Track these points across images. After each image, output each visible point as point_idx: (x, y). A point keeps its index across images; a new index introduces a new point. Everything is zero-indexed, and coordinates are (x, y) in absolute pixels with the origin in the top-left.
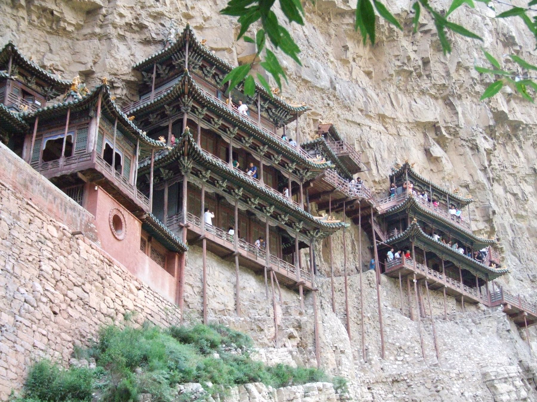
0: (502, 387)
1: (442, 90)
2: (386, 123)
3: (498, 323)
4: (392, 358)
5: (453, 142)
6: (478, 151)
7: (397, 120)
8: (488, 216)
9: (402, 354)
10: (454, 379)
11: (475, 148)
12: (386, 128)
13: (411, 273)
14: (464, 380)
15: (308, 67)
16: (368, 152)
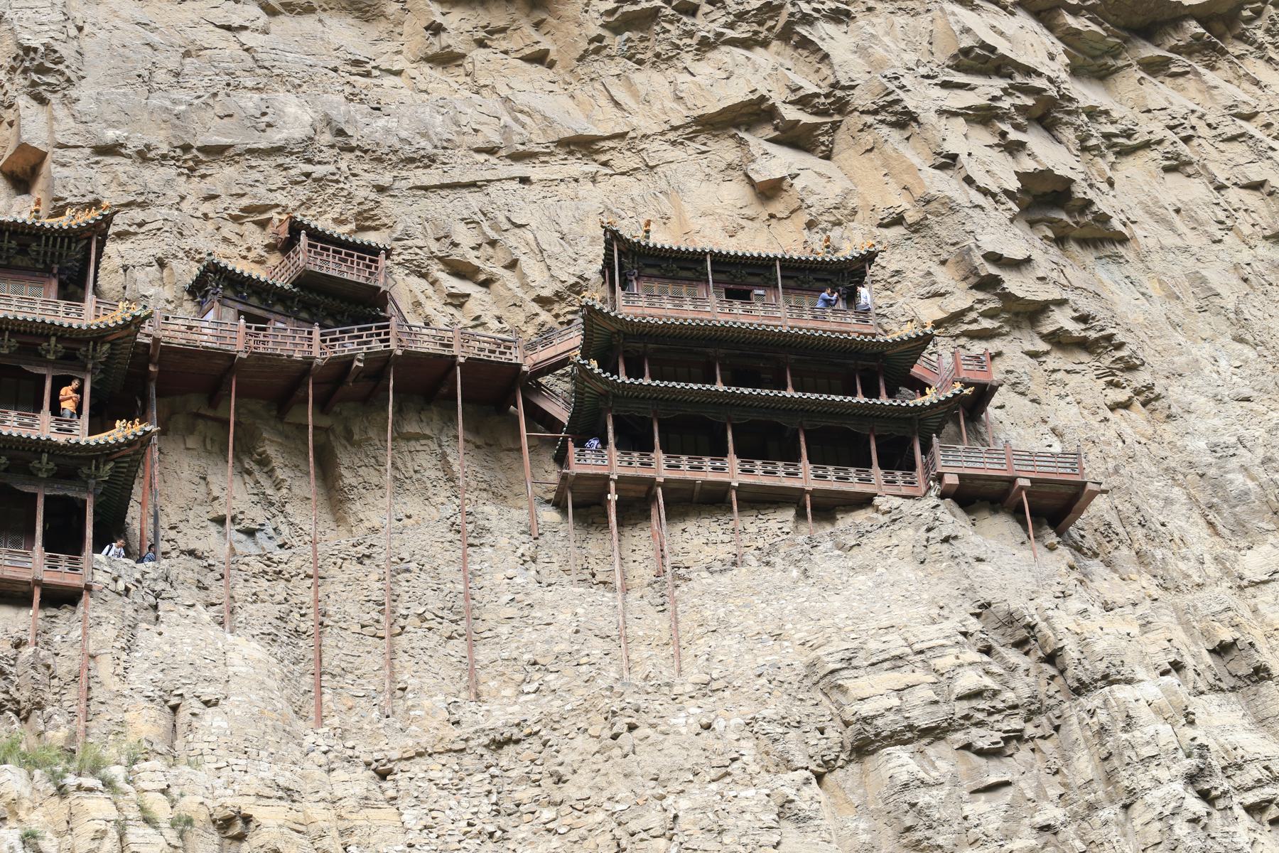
0: (859, 684)
1: (771, 18)
2: (598, 152)
3: (917, 530)
4: (509, 691)
5: (843, 127)
6: (919, 124)
7: (632, 134)
8: (974, 271)
9: (537, 676)
10: (686, 697)
11: (905, 120)
12: (605, 164)
13: (606, 479)
14: (727, 693)
15: (230, 116)
16: (511, 239)
